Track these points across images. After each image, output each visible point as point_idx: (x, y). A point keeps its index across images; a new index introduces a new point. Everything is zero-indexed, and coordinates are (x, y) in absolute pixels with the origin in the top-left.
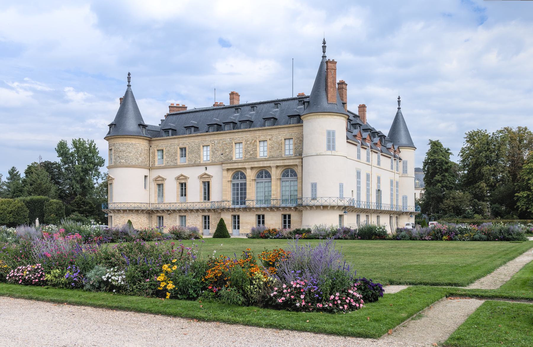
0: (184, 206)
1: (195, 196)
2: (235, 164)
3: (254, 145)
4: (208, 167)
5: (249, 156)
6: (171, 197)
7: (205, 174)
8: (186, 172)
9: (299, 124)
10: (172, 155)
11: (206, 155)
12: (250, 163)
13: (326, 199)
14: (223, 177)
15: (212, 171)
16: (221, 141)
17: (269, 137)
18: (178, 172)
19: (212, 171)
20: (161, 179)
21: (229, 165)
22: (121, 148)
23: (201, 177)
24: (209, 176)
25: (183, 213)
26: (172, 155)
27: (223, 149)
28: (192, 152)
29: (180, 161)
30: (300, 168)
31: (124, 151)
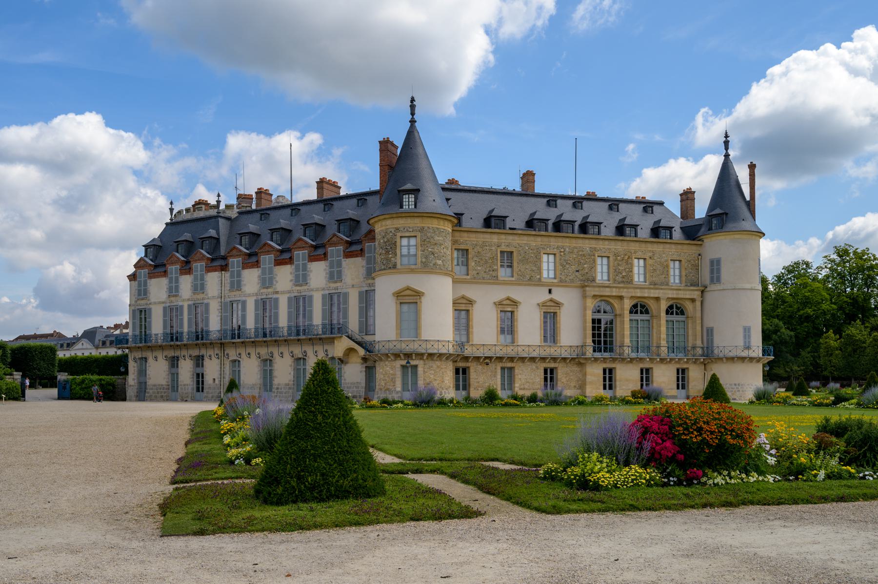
0: (510, 351)
1: (529, 333)
2: (608, 289)
3: (627, 263)
4: (554, 290)
5: (620, 280)
6: (485, 333)
7: (551, 300)
8: (516, 293)
9: (700, 243)
10: (486, 262)
11: (548, 267)
12: (630, 290)
13: (383, 344)
14: (585, 309)
15: (559, 294)
16: (576, 250)
17: (650, 254)
18: (500, 293)
19: (559, 294)
20: (465, 301)
21: (597, 289)
22: (436, 238)
23: (543, 305)
24: (558, 304)
25: (508, 364)
26: (486, 262)
27: (580, 263)
28: (524, 260)
29: (503, 273)
30: (698, 304)
31: (441, 245)
